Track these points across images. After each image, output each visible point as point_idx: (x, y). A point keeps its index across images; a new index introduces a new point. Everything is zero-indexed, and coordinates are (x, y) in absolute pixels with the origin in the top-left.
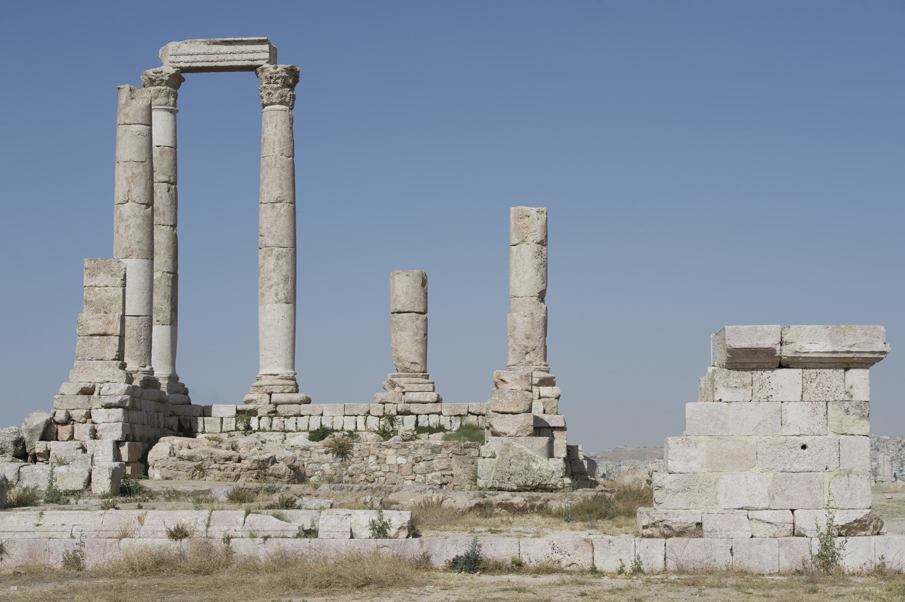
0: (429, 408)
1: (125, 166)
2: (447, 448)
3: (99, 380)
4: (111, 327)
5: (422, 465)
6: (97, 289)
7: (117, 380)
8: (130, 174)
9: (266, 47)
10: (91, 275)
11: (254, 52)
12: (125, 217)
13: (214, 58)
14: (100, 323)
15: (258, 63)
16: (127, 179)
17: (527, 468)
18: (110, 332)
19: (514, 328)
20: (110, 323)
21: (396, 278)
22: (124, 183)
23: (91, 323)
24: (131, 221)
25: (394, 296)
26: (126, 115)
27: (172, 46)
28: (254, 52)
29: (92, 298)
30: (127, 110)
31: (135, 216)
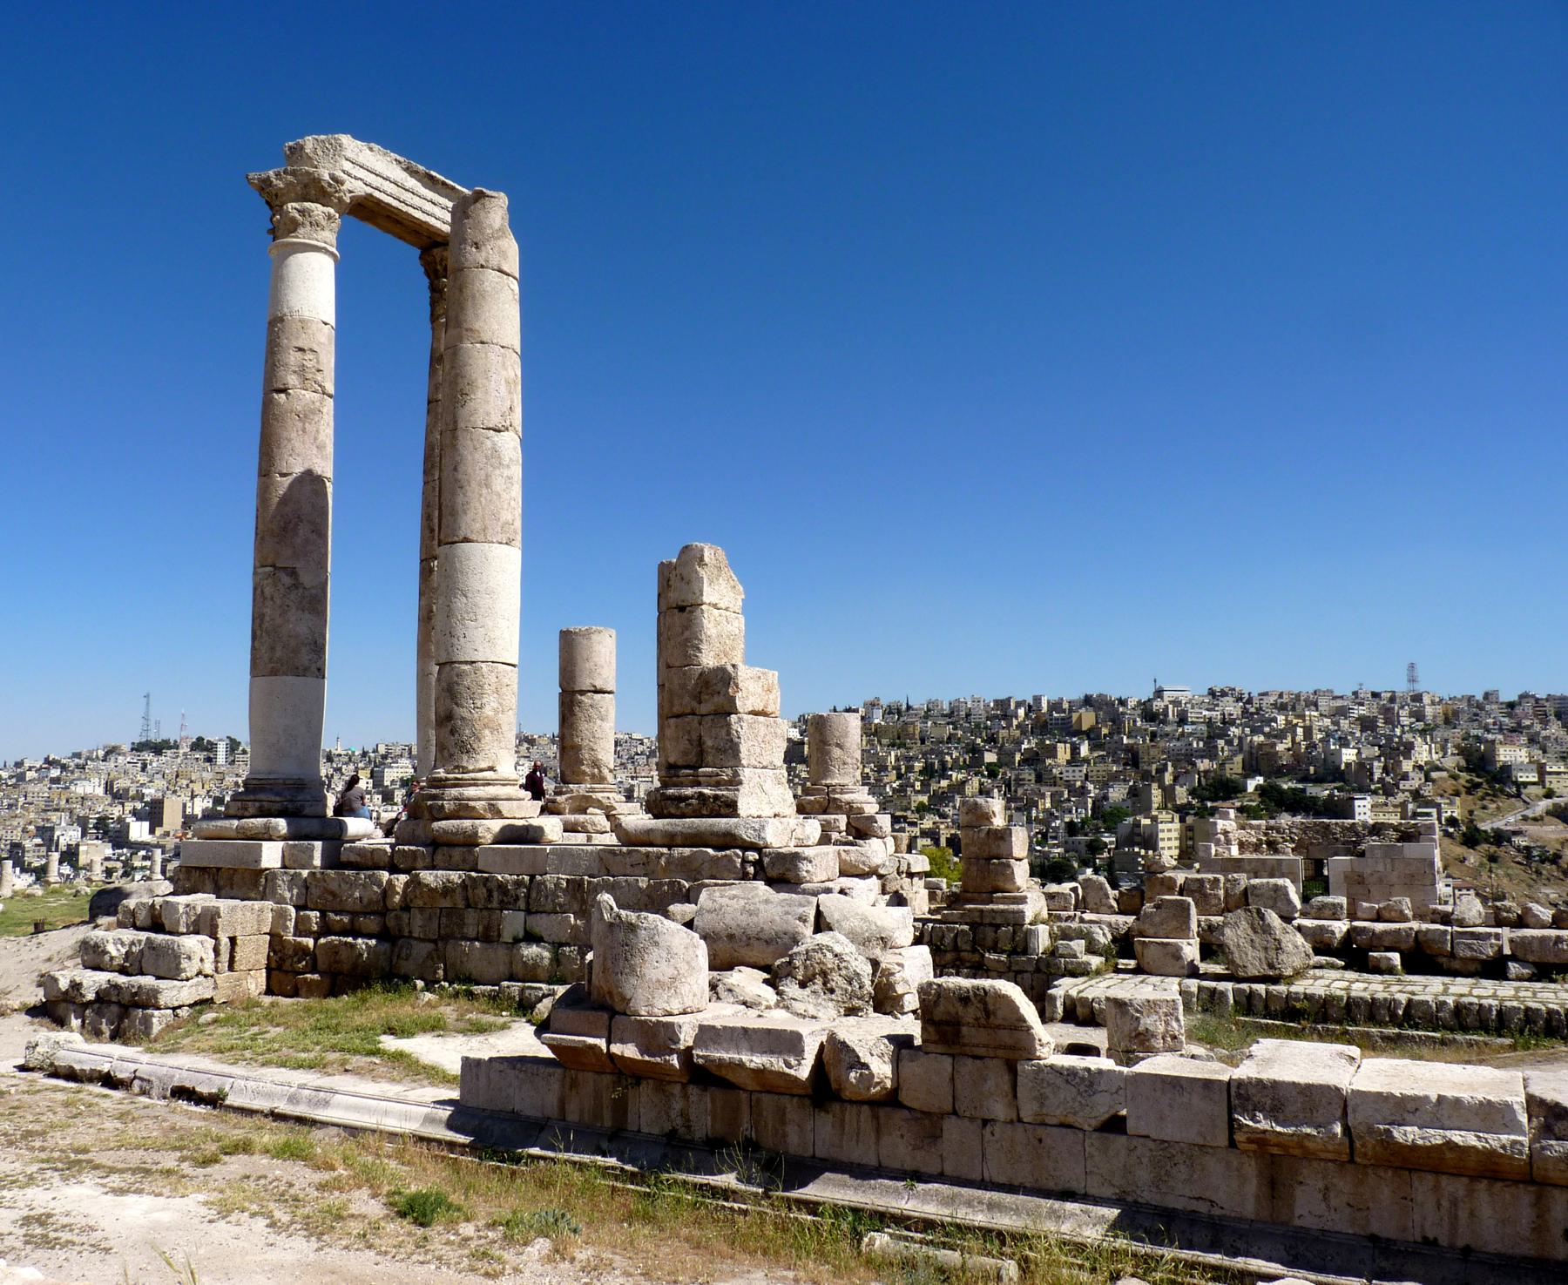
13: (407, 196)
18: (769, 710)
19: (846, 735)
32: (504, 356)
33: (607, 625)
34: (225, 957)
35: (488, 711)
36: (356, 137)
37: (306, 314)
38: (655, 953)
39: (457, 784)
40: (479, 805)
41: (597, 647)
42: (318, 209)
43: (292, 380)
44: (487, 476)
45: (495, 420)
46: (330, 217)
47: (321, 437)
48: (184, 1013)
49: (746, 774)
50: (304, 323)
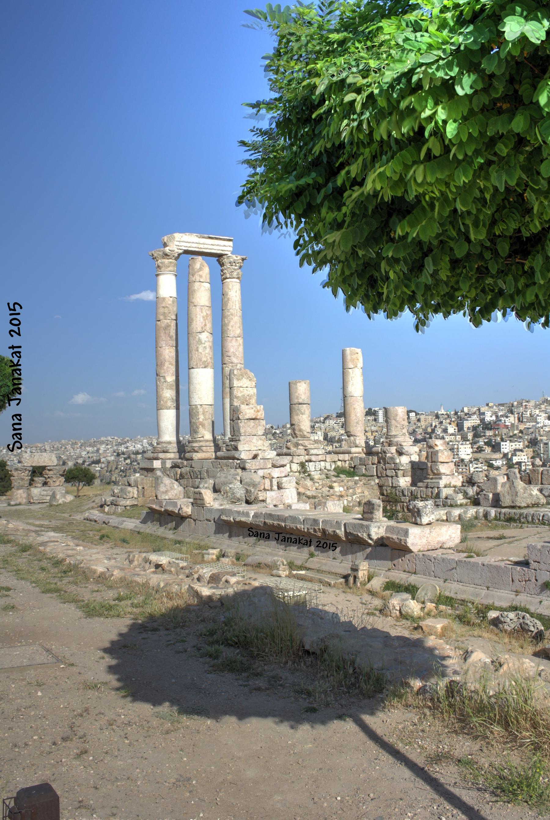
0: (320, 458)
1: (202, 309)
2: (361, 481)
3: (255, 448)
4: (259, 414)
5: (351, 491)
6: (241, 389)
7: (265, 448)
8: (205, 314)
9: (231, 243)
10: (238, 380)
11: (225, 246)
12: (203, 342)
13: (202, 246)
14: (252, 411)
15: (226, 253)
16: (203, 317)
17: (531, 495)
19: (397, 415)
20: (258, 411)
21: (298, 384)
22: (202, 320)
23: (248, 411)
24: (207, 345)
25: (297, 394)
26: (201, 276)
27: (177, 236)
28: (225, 246)
29: (239, 395)
30: (201, 273)
31: (209, 341)
32: (202, 309)
33: (303, 379)
34: (141, 493)
35: (201, 420)
36: (180, 233)
37: (164, 296)
38: (162, 485)
39: (193, 442)
40: (196, 449)
41: (299, 388)
42: (166, 261)
43: (161, 317)
44: (197, 348)
45: (199, 329)
46: (171, 262)
47: (171, 334)
48: (128, 508)
49: (242, 438)
50: (164, 299)
